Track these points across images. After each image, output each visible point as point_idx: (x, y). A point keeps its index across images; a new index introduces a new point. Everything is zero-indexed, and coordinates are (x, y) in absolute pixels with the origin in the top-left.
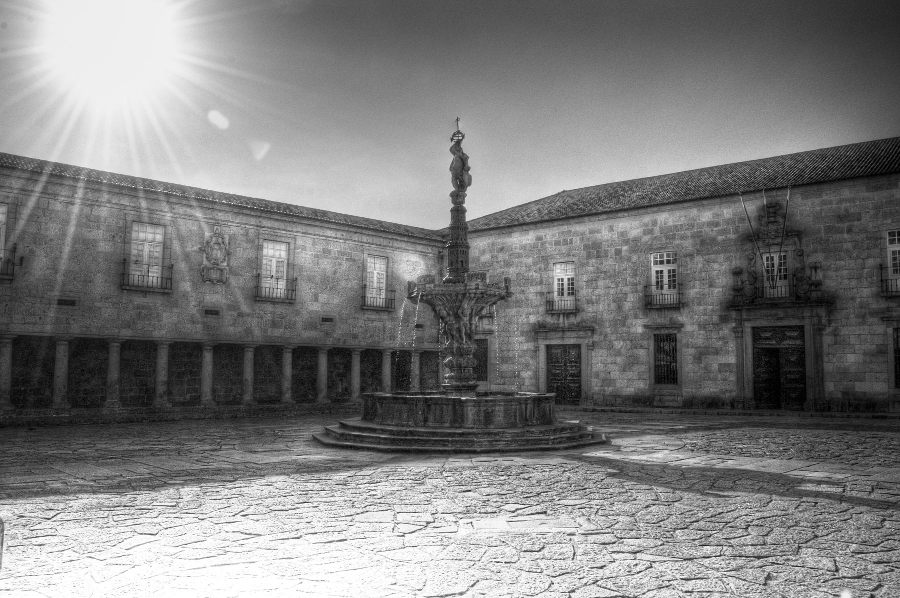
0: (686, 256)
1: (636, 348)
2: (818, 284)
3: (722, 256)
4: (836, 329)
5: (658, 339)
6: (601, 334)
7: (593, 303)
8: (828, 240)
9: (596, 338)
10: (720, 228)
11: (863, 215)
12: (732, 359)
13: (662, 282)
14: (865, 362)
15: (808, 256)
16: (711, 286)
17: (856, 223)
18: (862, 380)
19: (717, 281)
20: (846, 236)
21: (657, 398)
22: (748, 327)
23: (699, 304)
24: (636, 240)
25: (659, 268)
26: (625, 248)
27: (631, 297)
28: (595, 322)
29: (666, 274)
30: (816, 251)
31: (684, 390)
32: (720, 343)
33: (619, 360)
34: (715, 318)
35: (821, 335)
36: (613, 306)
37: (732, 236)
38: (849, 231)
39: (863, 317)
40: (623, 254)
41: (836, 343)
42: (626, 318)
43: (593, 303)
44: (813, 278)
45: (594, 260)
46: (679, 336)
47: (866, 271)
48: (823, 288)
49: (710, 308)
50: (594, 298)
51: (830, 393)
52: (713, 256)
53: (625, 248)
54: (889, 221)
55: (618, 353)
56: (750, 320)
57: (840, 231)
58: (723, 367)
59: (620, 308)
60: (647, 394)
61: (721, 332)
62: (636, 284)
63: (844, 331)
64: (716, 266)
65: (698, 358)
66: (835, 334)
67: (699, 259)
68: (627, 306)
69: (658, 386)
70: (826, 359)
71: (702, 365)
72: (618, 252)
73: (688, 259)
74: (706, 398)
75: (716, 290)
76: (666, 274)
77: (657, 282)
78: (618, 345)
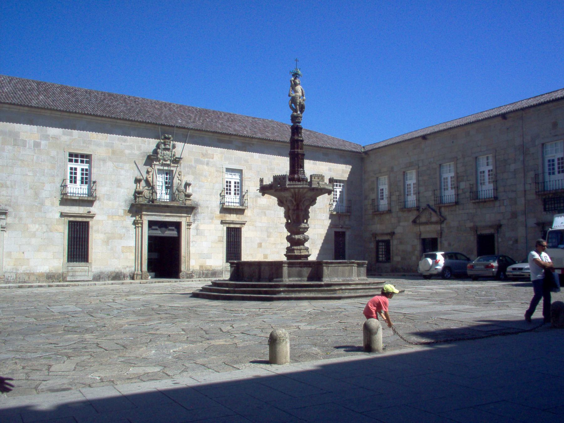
0: (100, 160)
1: (51, 232)
2: (188, 196)
3: (128, 165)
4: (198, 225)
5: (72, 225)
6: (15, 218)
7: (7, 187)
8: (195, 168)
9: (9, 220)
10: (128, 144)
11: (215, 156)
12: (132, 243)
13: (75, 178)
14: (212, 247)
15: (184, 176)
16: (118, 187)
17: (211, 160)
18: (210, 258)
19: (123, 184)
20: (205, 167)
21: (70, 274)
22: (146, 219)
23: (109, 199)
24: (55, 138)
25: (73, 165)
26: (43, 142)
27: (48, 187)
28: (10, 206)
29: (79, 172)
30: (189, 174)
31: (93, 267)
32: (124, 230)
33: (33, 241)
34: (121, 212)
35: (190, 229)
36: (30, 192)
37: (137, 152)
38: (207, 164)
39: (212, 219)
40: (42, 147)
41: (197, 235)
42: (42, 204)
43: (7, 187)
44: (188, 191)
45: (10, 147)
46: (91, 223)
47: (214, 191)
48: (192, 198)
49: (117, 203)
50: (8, 183)
51: (193, 266)
52: (121, 164)
53: (43, 142)
54: (227, 162)
55: (34, 235)
56: (148, 215)
57: (202, 163)
58: (126, 249)
59: (37, 194)
60: (61, 271)
61: (124, 222)
62: (53, 176)
63: (202, 227)
64: (123, 172)
65: (107, 242)
66: (197, 229)
67: (110, 164)
68: (44, 194)
69: (72, 264)
70: (191, 244)
71: (109, 247)
72: (37, 145)
73: (102, 163)
74: (111, 273)
75: (122, 190)
76: (79, 172)
77: (71, 177)
78: (33, 228)
